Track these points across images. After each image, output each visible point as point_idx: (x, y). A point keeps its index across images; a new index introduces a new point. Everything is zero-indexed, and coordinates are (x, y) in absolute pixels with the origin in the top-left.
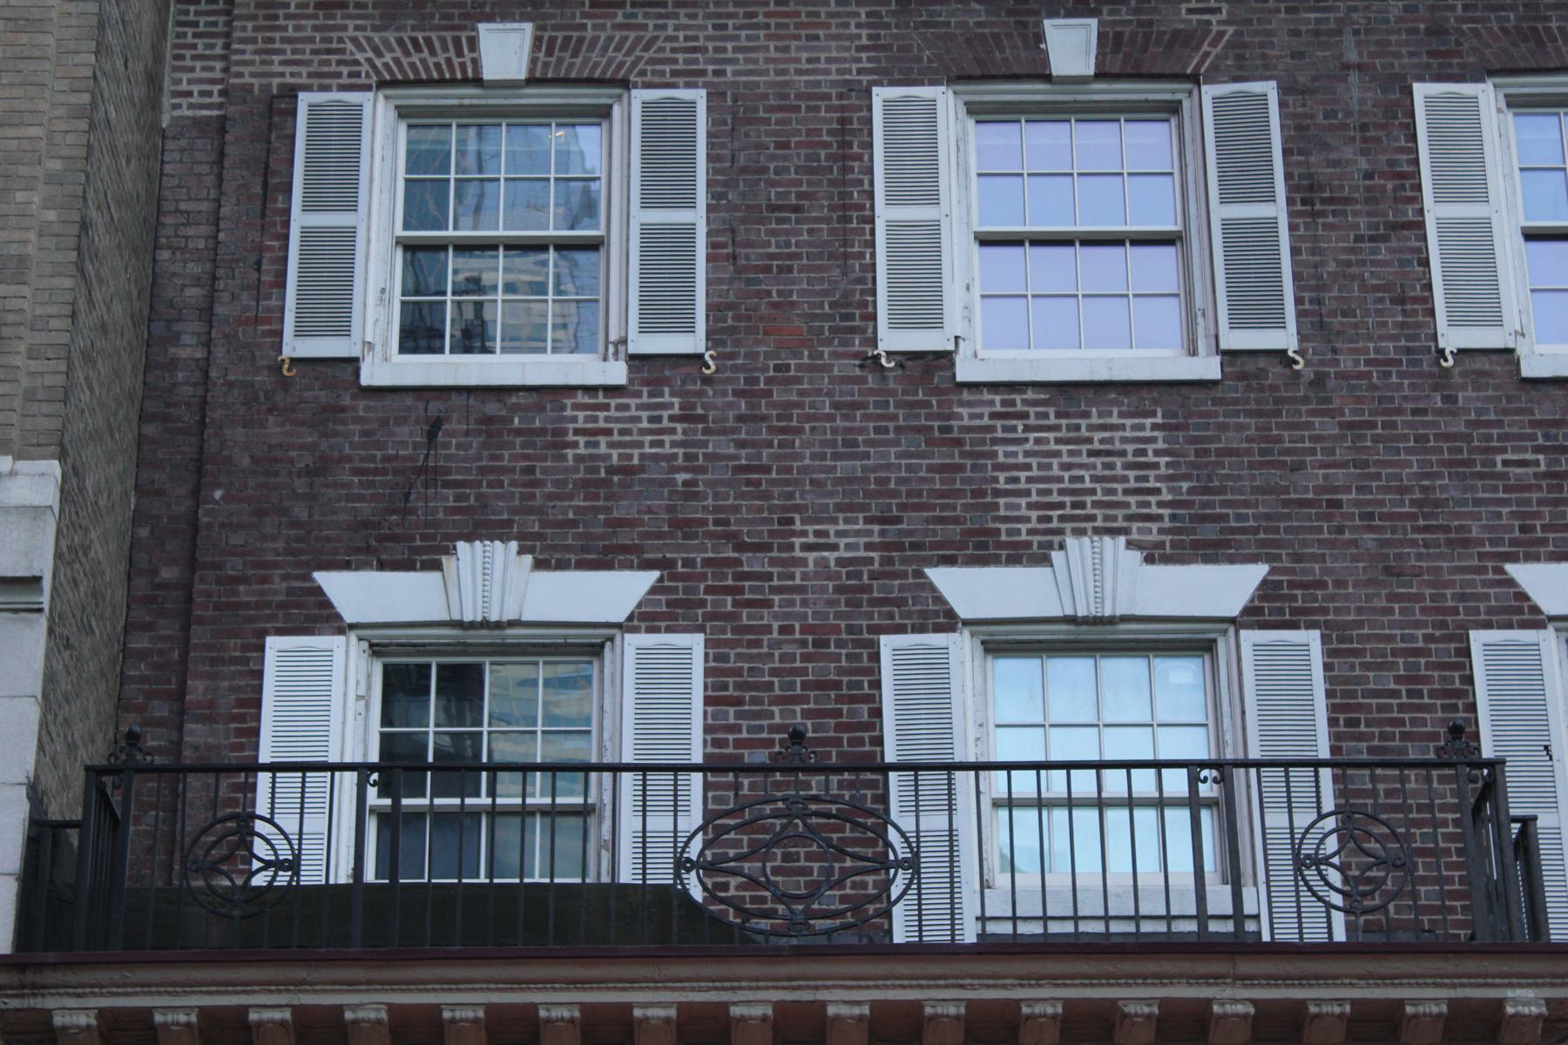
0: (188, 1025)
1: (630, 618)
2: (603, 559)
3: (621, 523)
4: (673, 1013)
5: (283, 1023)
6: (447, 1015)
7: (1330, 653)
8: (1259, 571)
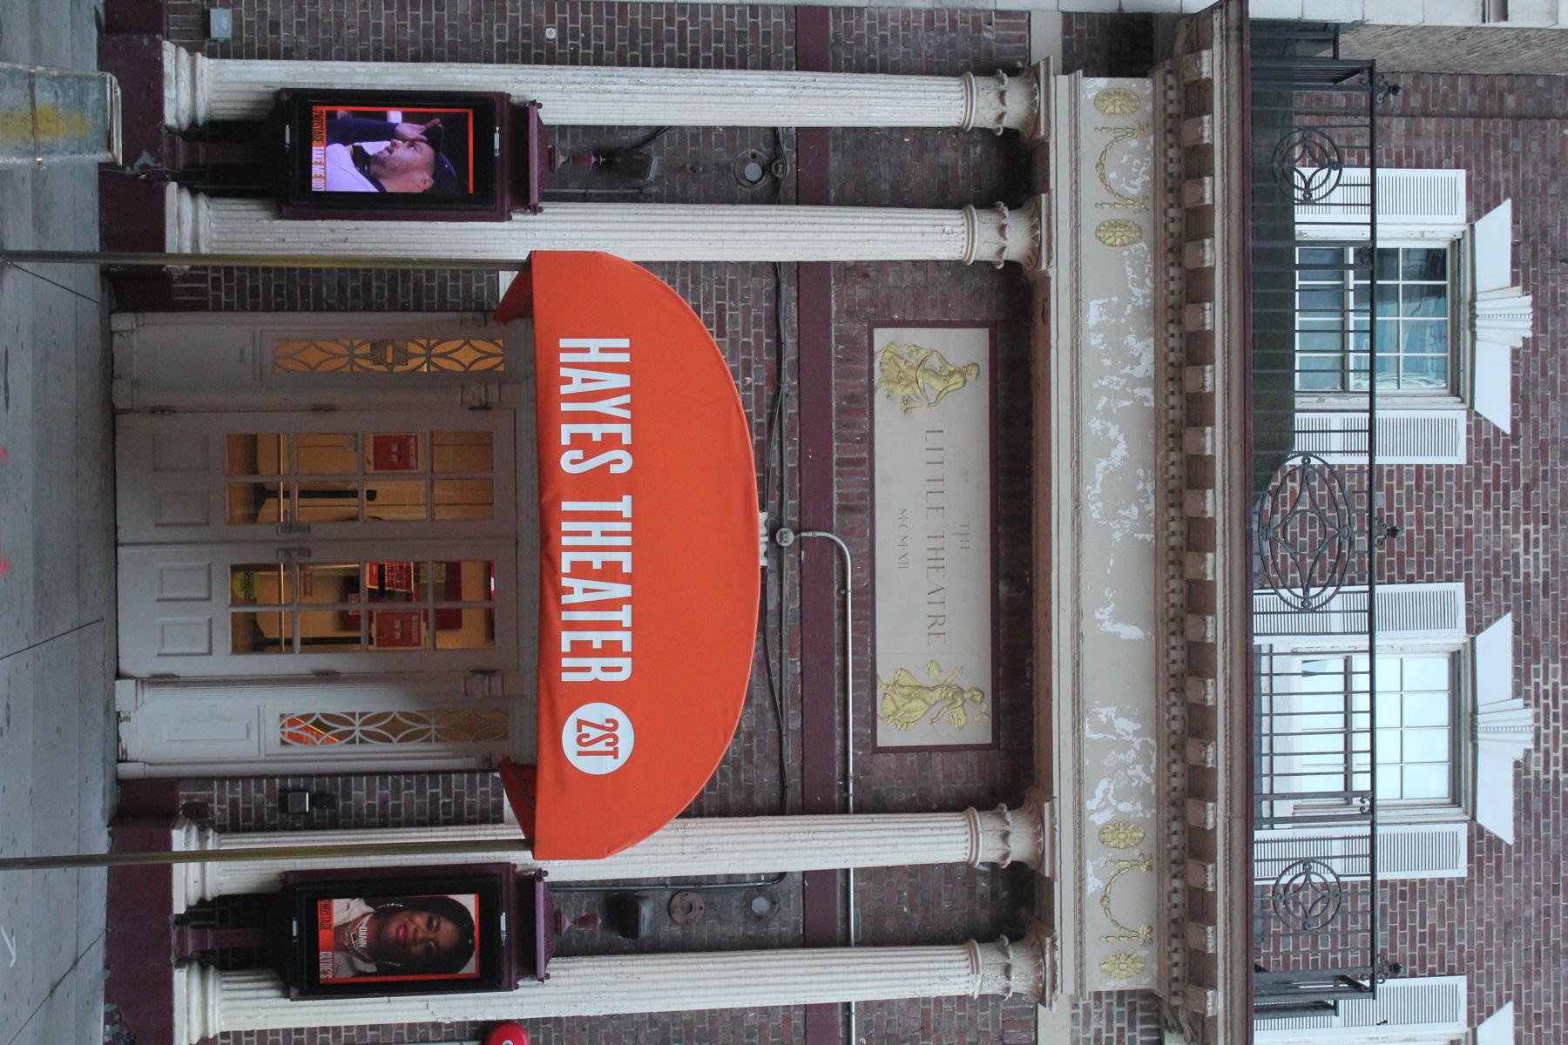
0: (1202, 138)
1: (1477, 414)
2: (1520, 394)
3: (1545, 407)
4: (1208, 452)
5: (1202, 199)
6: (1208, 305)
7: (1451, 883)
8: (1508, 837)
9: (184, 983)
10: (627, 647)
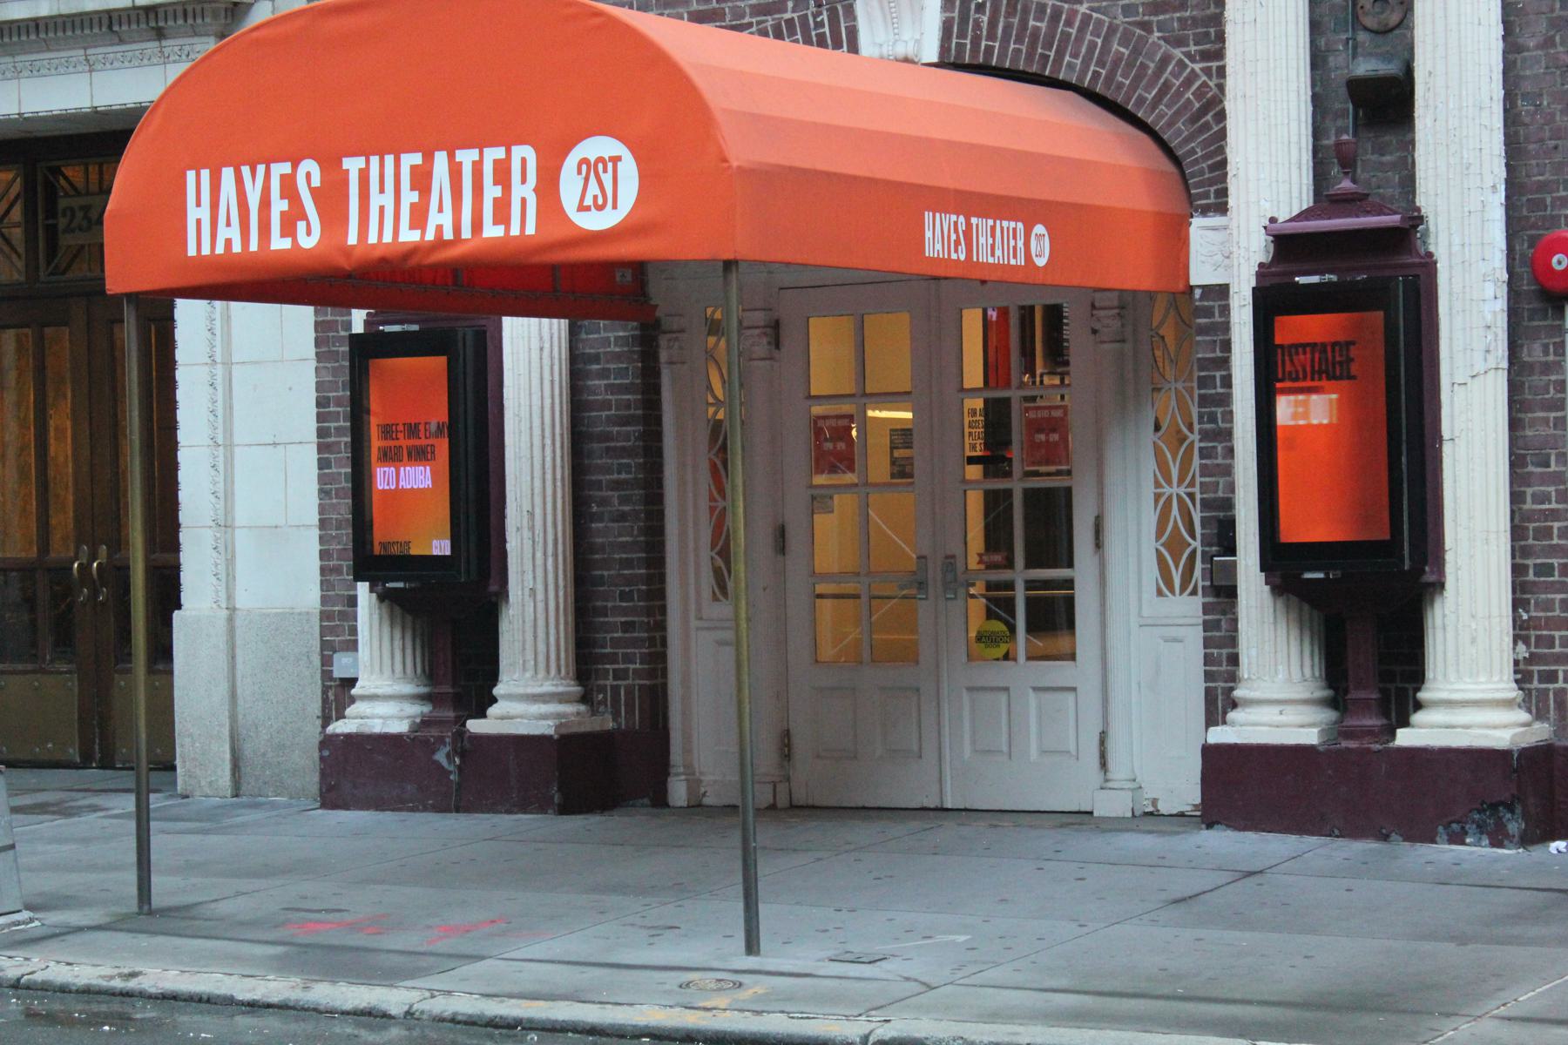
9: (1421, 733)
10: (500, 153)
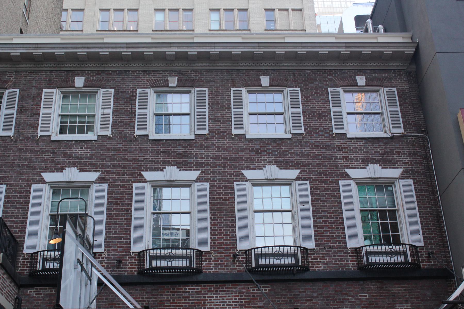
7: (8, 189)
